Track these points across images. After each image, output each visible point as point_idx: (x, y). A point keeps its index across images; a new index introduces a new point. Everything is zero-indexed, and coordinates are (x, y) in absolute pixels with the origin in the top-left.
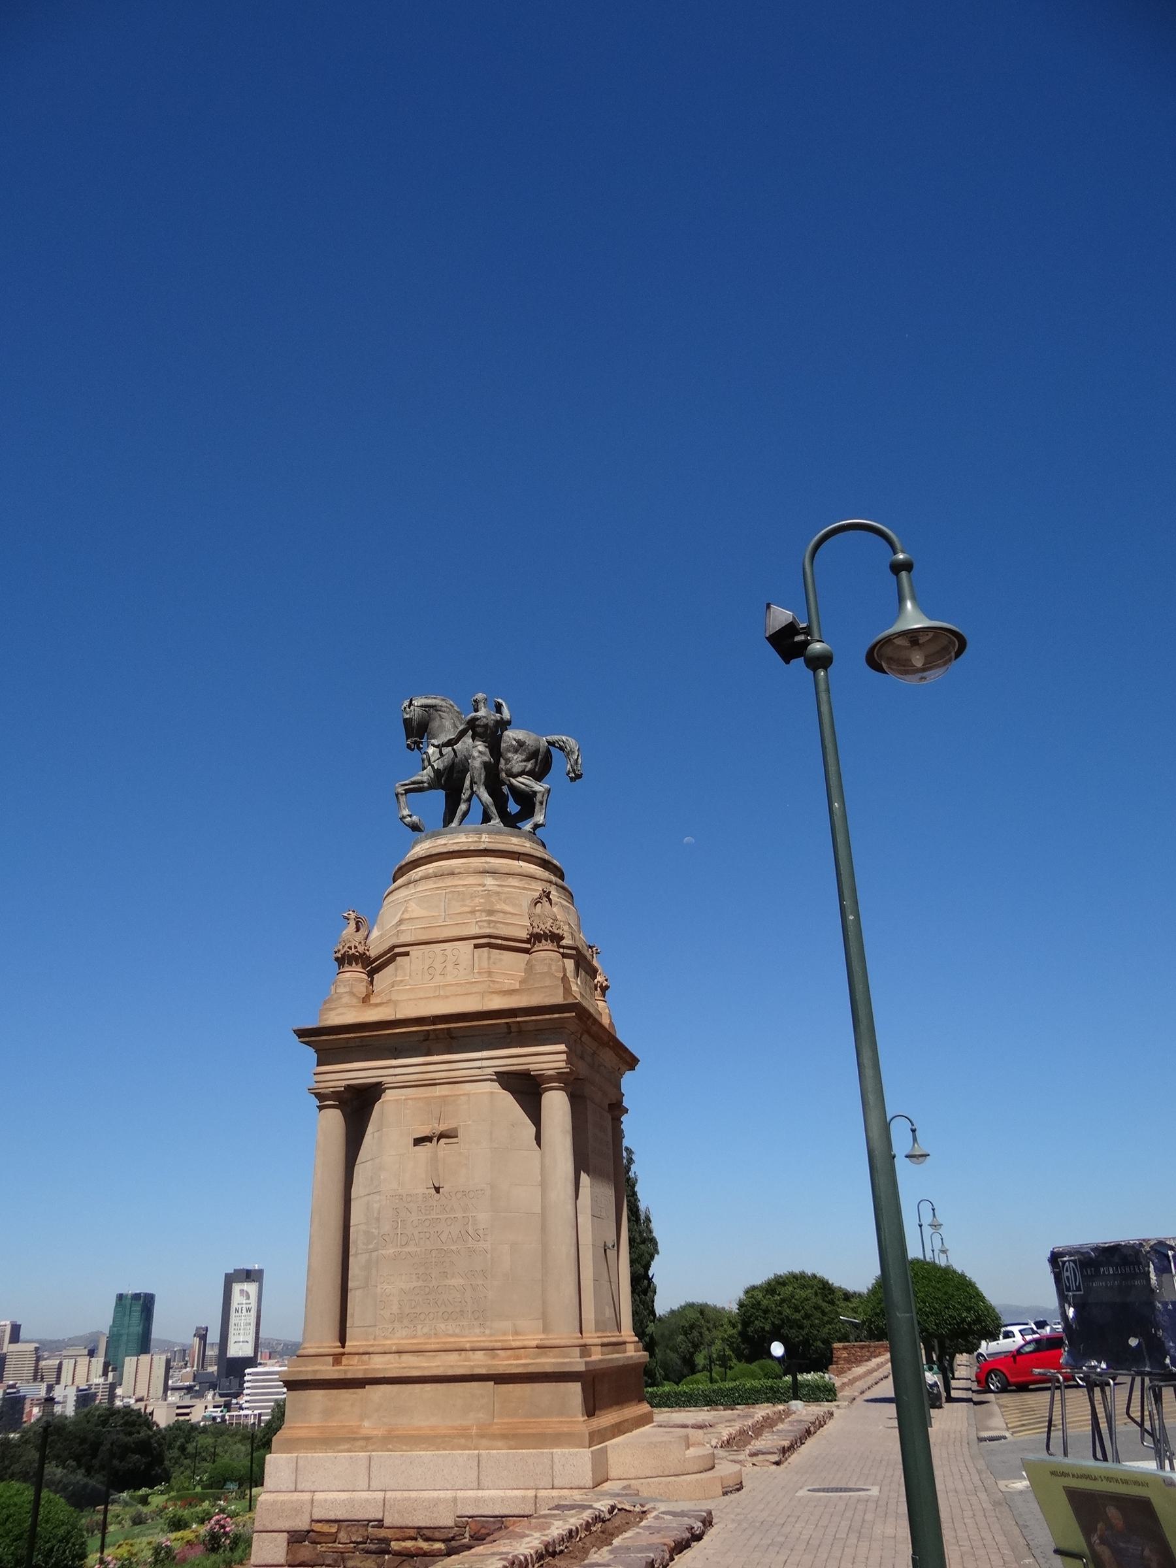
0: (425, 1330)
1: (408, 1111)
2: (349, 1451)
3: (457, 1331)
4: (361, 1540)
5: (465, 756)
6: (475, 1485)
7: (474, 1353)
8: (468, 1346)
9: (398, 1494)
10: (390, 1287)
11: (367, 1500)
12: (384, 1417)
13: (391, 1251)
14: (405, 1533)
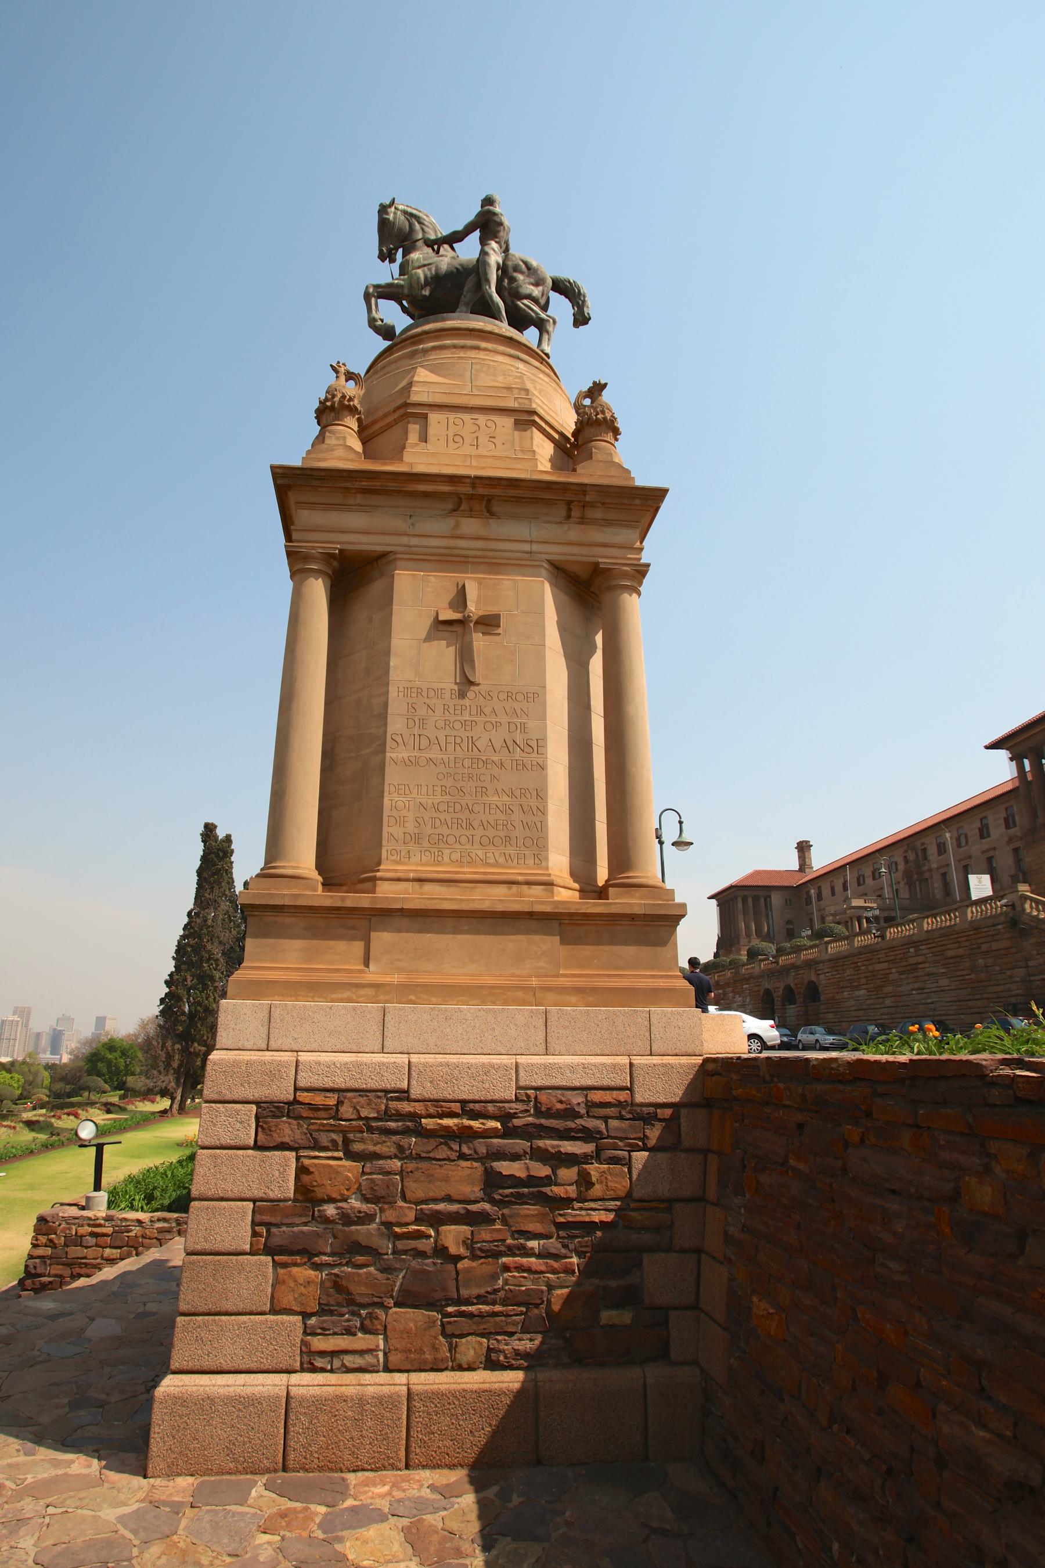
0: (456, 856)
1: (429, 589)
2: (350, 1000)
3: (502, 860)
4: (376, 1115)
5: (457, 269)
6: (541, 1049)
7: (529, 888)
8: (520, 878)
9: (430, 1059)
10: (404, 799)
11: (381, 1065)
12: (399, 960)
13: (405, 755)
14: (440, 1107)
